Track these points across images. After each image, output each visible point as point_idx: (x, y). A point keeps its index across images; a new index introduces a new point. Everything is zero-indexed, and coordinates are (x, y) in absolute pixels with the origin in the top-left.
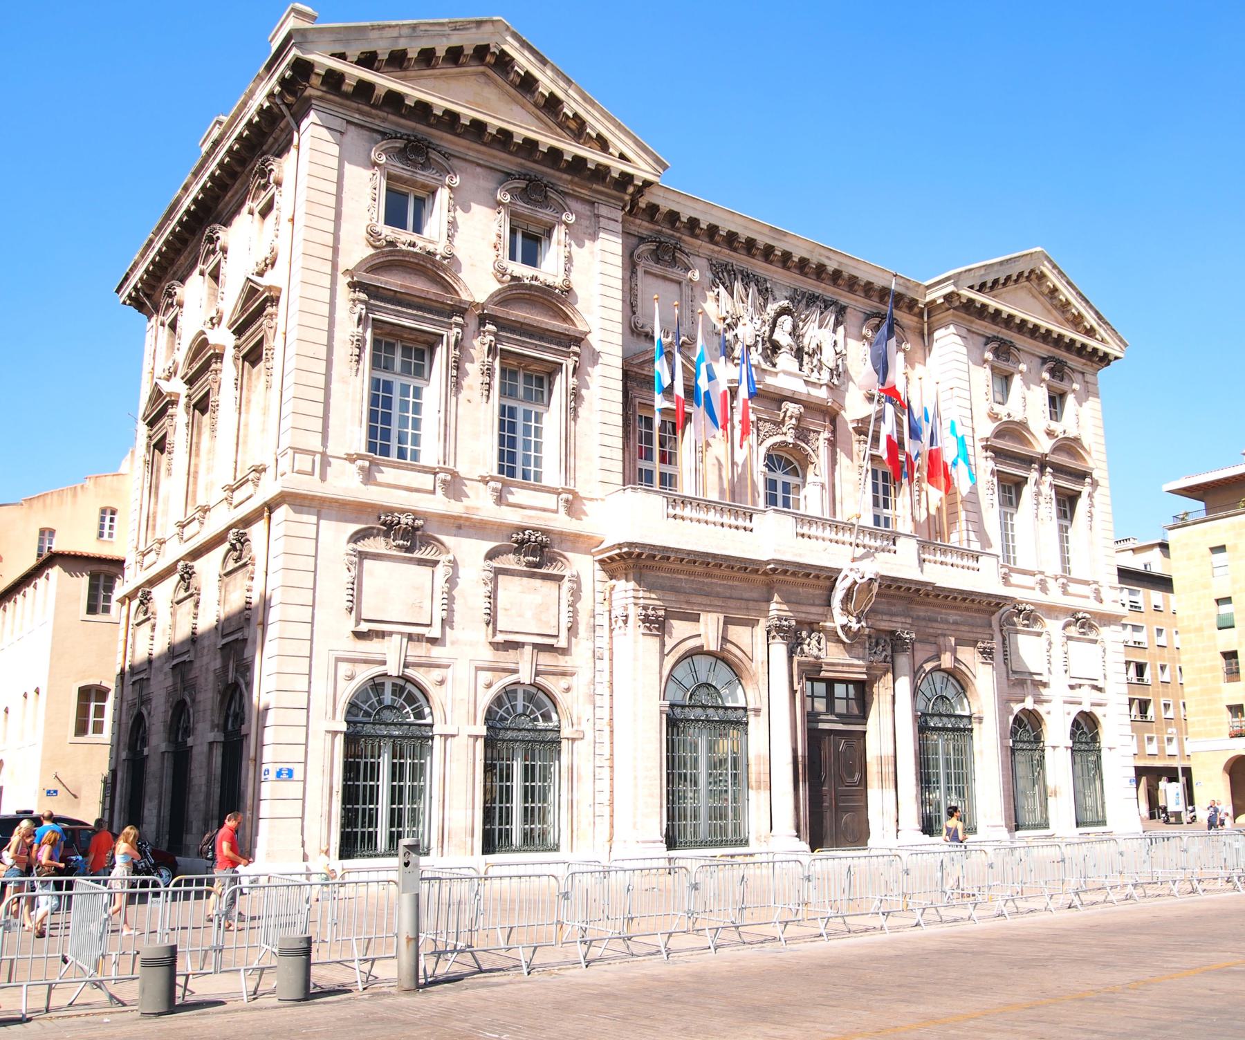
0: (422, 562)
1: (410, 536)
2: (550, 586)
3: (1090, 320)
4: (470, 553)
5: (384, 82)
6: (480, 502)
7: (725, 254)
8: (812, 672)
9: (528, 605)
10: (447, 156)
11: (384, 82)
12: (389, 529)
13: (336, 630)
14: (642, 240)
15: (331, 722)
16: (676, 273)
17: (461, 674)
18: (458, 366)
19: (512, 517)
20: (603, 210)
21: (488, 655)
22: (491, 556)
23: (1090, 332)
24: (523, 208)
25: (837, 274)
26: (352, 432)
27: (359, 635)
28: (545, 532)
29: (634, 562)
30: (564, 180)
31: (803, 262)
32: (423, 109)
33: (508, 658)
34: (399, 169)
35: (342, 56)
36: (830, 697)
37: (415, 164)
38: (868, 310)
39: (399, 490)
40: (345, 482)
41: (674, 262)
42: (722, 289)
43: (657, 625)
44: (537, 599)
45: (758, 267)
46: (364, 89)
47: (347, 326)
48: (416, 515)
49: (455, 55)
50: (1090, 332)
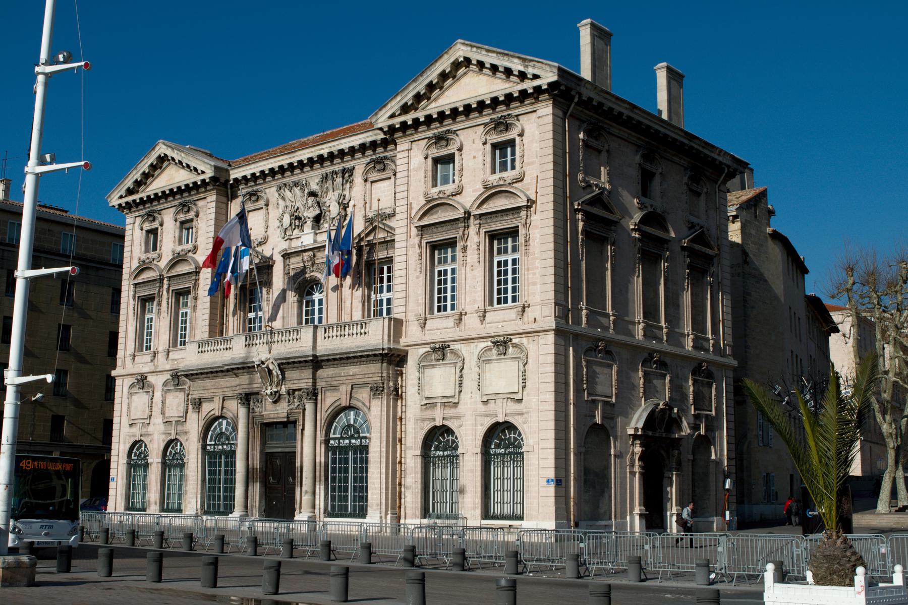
2: (182, 393)
3: (516, 66)
18: (159, 304)
19: (168, 367)
21: (162, 427)
23: (522, 76)
35: (121, 197)
38: (367, 160)
44: (177, 401)
45: (298, 176)
48: (142, 375)
50: (522, 76)
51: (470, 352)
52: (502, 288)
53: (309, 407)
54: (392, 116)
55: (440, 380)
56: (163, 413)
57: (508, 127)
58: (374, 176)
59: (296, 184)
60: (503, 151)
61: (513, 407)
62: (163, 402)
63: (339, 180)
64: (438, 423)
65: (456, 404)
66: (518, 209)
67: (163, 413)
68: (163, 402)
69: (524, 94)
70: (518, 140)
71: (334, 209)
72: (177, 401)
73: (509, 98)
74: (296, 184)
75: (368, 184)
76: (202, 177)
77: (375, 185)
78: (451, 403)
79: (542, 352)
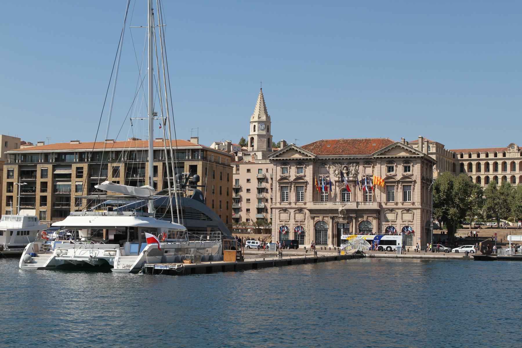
1: (285, 210)
3: (413, 151)
4: (292, 211)
6: (293, 205)
8: (338, 223)
9: (299, 217)
12: (283, 210)
13: (278, 221)
15: (277, 231)
17: (292, 225)
18: (291, 189)
19: (296, 206)
21: (294, 223)
24: (298, 166)
26: (279, 200)
29: (311, 211)
30: (304, 161)
33: (297, 223)
39: (285, 205)
40: (278, 205)
43: (313, 218)
47: (278, 188)
49: (287, 151)
53: (354, 221)
55: (390, 216)
56: (295, 219)
57: (409, 163)
58: (365, 166)
59: (340, 163)
60: (407, 169)
61: (410, 223)
62: (295, 216)
63: (355, 165)
64: (390, 225)
67: (295, 219)
68: (295, 216)
69: (415, 157)
71: (353, 172)
73: (411, 157)
77: (367, 168)
79: (418, 213)
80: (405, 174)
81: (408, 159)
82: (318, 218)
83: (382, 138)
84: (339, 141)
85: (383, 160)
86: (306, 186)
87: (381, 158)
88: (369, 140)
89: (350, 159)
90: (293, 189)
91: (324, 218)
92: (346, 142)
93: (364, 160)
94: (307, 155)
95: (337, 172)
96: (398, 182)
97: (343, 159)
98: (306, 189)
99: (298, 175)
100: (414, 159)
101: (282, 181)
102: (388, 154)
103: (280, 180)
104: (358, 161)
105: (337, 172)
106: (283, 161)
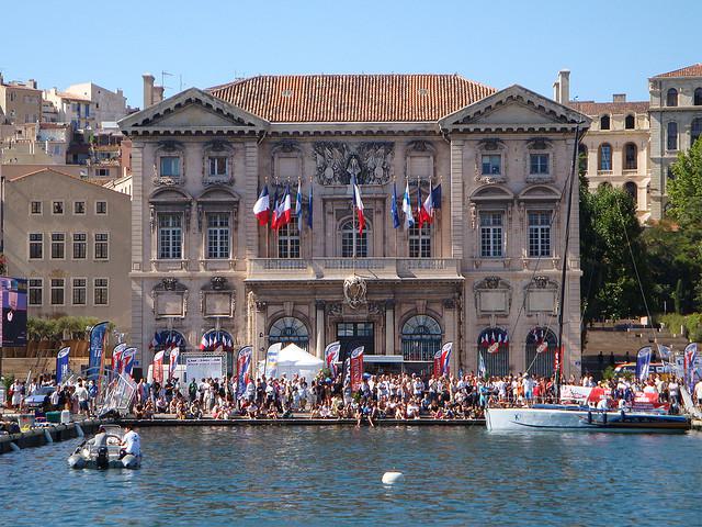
0: (178, 294)
5: (151, 129)
7: (319, 139)
9: (220, 307)
10: (180, 144)
11: (151, 129)
14: (277, 144)
16: (295, 153)
18: (188, 222)
19: (210, 274)
20: (248, 145)
22: (203, 289)
24: (213, 154)
25: (380, 132)
27: (157, 319)
28: (222, 278)
30: (229, 139)
31: (358, 132)
32: (167, 133)
34: (163, 154)
35: (136, 125)
36: (355, 330)
37: (169, 151)
41: (293, 150)
42: (319, 156)
45: (340, 139)
46: (145, 133)
51: (518, 287)
52: (539, 246)
54: (457, 123)
55: (493, 301)
60: (540, 164)
63: (382, 151)
64: (493, 326)
65: (506, 316)
66: (554, 201)
67: (204, 311)
68: (204, 303)
70: (551, 156)
72: (218, 304)
73: (553, 130)
74: (336, 145)
75: (408, 159)
76: (252, 128)
78: (502, 315)
80: (535, 176)
81: (544, 135)
82: (279, 308)
83: (438, 72)
84: (310, 80)
85: (469, 137)
86: (236, 214)
87: (467, 131)
88: (402, 77)
89: (369, 133)
90: (194, 222)
91: (299, 308)
92: (333, 80)
93: (409, 139)
94: (240, 122)
95: (329, 173)
96: (516, 201)
97: (349, 133)
98: (236, 223)
99: (212, 179)
100: (560, 136)
101: (161, 199)
102: (483, 119)
103: (156, 195)
104: (392, 139)
105: (329, 173)
106: (166, 138)
